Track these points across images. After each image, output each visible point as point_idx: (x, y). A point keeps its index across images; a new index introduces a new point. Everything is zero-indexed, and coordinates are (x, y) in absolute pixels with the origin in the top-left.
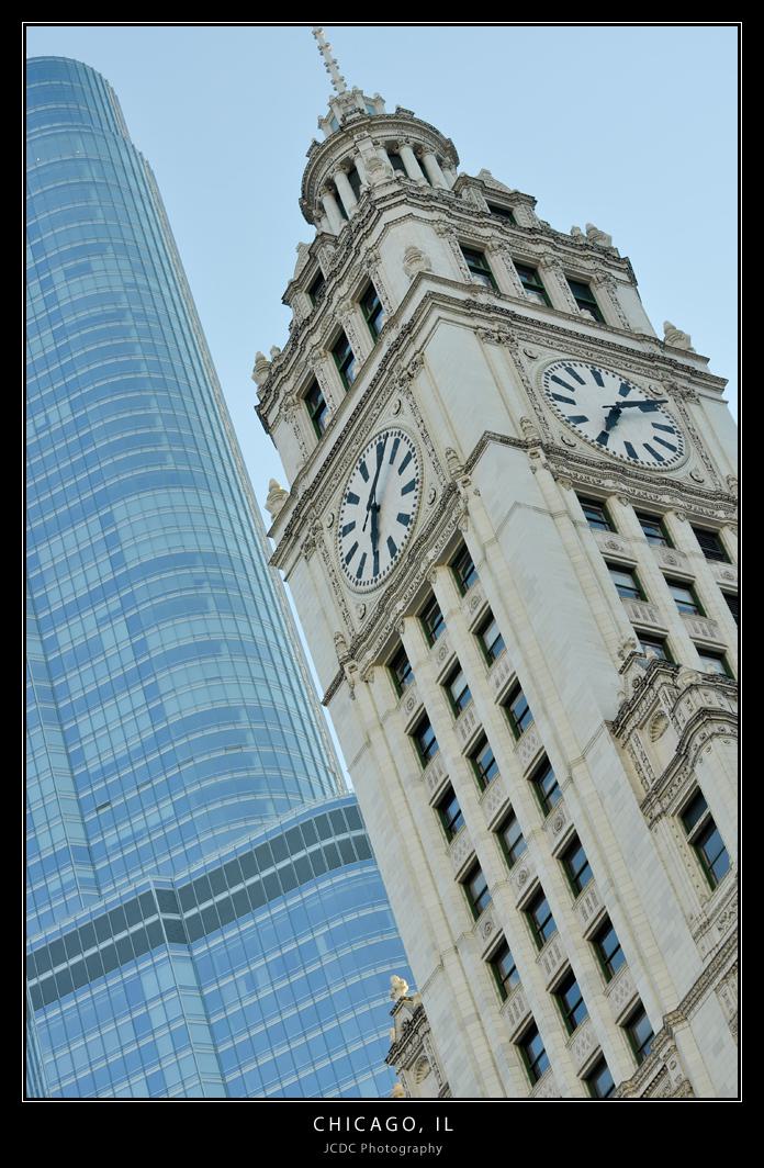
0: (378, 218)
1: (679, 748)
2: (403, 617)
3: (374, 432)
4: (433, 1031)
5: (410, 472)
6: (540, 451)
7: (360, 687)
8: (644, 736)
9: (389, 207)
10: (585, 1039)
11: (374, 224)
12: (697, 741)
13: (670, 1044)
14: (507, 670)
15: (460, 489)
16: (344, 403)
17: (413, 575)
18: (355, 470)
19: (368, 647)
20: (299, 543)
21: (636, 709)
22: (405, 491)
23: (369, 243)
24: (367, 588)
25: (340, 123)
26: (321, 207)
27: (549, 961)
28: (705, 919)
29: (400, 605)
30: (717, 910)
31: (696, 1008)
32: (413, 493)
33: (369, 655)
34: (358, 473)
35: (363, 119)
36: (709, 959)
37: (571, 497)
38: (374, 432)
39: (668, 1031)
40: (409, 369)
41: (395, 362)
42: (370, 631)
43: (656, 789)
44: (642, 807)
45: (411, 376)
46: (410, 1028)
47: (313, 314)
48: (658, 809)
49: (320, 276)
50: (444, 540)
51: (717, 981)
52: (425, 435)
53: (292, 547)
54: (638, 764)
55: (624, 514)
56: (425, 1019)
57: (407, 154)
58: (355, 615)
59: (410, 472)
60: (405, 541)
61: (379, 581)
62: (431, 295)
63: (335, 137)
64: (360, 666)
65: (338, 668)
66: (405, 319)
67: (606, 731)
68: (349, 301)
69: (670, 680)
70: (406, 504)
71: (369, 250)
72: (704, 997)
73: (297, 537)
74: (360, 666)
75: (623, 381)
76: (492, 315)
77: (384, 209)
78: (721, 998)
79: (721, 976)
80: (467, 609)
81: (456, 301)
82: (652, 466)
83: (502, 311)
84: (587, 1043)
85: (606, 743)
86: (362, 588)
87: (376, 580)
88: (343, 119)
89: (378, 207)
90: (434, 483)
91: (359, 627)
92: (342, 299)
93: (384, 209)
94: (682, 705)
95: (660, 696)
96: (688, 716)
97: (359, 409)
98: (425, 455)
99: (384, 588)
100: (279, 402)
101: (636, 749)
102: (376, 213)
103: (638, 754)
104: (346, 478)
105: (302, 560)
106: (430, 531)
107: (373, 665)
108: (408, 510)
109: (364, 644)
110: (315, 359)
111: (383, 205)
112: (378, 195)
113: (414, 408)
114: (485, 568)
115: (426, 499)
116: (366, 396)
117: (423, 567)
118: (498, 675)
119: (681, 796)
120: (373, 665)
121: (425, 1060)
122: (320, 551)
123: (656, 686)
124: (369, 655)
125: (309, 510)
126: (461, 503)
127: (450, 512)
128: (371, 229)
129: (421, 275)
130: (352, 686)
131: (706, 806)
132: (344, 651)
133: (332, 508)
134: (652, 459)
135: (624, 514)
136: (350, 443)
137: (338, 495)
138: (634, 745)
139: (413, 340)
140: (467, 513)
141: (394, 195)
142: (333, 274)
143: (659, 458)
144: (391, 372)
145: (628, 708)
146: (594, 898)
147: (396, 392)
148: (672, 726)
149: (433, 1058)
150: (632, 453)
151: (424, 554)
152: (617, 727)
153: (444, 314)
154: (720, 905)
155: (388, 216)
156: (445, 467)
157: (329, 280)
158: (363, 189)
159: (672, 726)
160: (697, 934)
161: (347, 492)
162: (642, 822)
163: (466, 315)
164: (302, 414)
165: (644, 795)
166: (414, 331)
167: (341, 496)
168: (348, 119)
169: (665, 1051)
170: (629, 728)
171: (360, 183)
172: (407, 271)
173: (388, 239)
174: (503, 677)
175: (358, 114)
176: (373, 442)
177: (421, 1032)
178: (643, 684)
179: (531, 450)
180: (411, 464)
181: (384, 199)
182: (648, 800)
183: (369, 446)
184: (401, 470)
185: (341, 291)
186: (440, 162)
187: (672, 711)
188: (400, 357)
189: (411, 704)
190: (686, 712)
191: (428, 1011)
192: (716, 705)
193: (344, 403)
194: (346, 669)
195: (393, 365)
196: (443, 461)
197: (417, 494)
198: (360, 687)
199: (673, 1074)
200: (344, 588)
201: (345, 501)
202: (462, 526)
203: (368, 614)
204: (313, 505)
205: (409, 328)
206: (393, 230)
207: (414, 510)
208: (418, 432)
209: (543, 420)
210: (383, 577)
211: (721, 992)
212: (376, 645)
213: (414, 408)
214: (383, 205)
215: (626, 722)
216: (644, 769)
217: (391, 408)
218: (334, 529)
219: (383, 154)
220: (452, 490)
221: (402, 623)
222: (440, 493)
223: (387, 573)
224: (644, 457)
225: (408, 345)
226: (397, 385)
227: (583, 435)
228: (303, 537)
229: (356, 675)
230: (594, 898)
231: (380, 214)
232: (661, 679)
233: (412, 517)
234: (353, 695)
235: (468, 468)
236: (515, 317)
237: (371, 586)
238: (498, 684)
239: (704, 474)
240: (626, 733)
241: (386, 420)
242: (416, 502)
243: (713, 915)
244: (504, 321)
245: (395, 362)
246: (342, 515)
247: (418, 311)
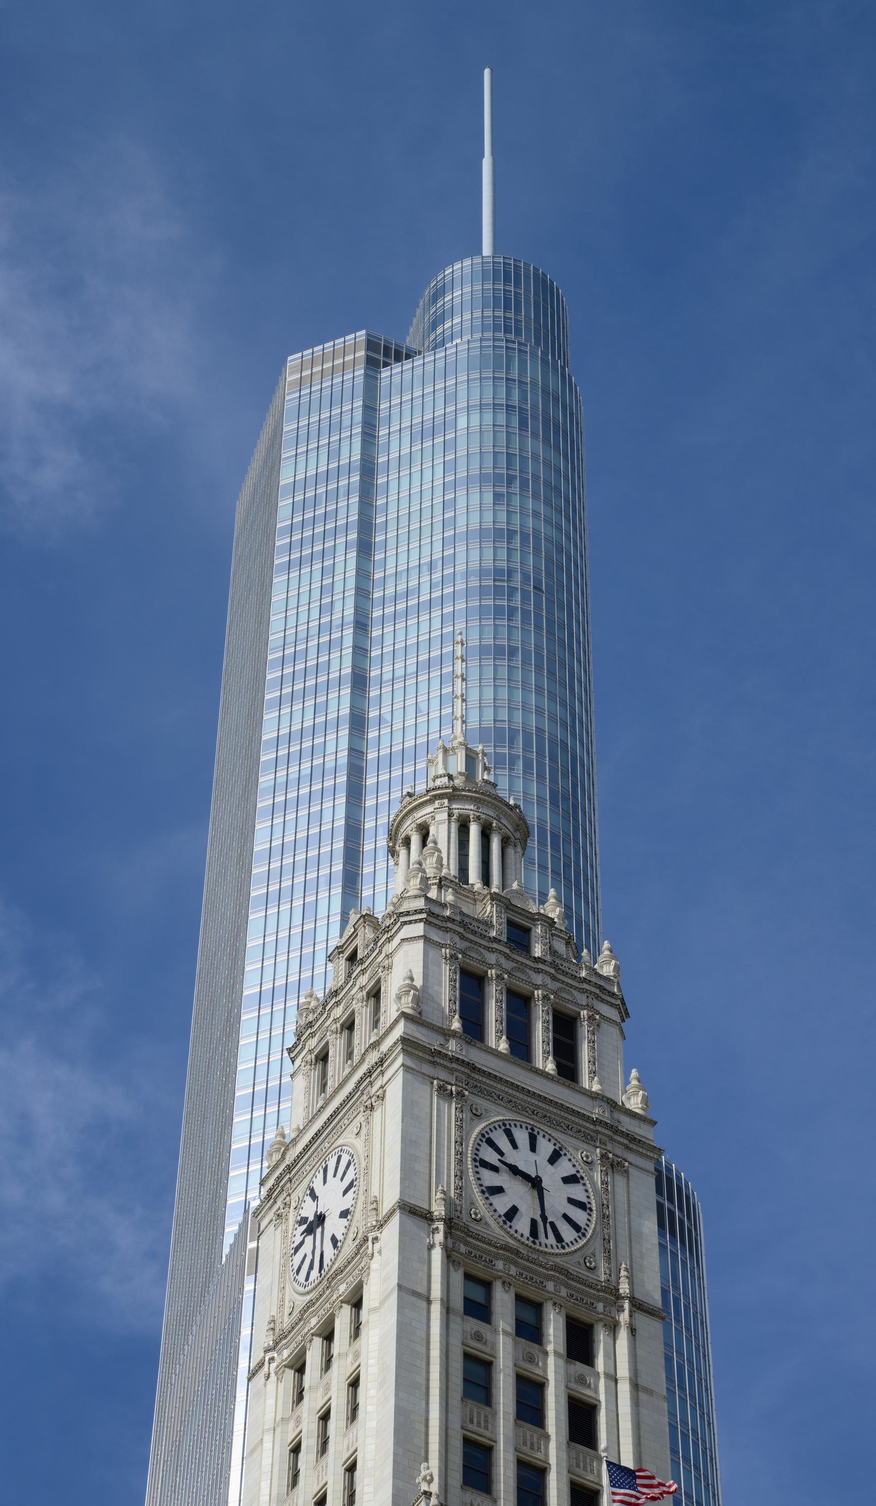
0: (399, 929)
2: (313, 1335)
9: (410, 922)
37: (458, 1277)
71: (387, 956)
76: (454, 1065)
77: (405, 923)
89: (402, 919)
102: (399, 924)
107: (286, 1366)
109: (284, 1342)
120: (286, 1366)
130: (268, 1377)
141: (416, 912)
163: (431, 1062)
181: (408, 913)
206: (406, 946)
212: (294, 1345)
244: (463, 1073)
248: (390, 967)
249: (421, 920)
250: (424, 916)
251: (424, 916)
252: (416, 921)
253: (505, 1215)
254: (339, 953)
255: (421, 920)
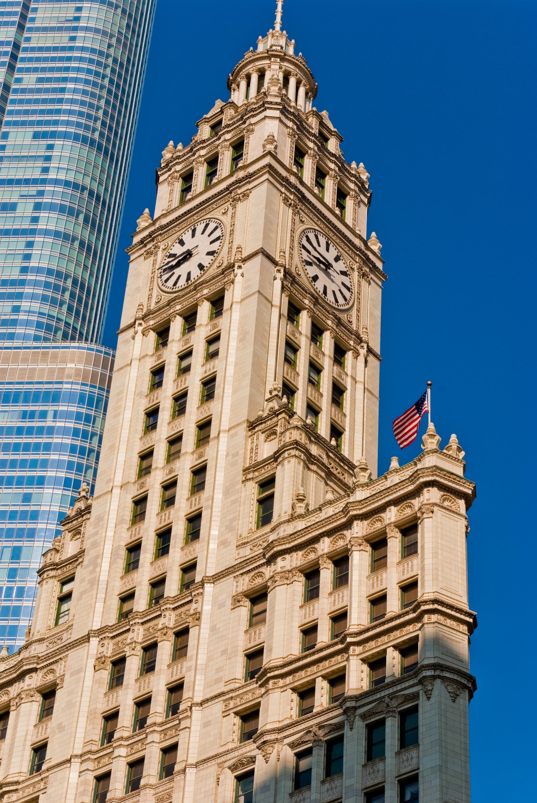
0: (263, 111)
1: (275, 453)
2: (177, 314)
3: (208, 216)
4: (91, 520)
5: (215, 246)
6: (282, 271)
7: (139, 336)
8: (262, 437)
9: (271, 108)
10: (161, 565)
11: (260, 112)
12: (286, 454)
13: (201, 590)
14: (213, 368)
15: (236, 268)
16: (201, 194)
17: (192, 297)
18: (189, 229)
19: (153, 319)
20: (144, 249)
21: (265, 422)
22: (209, 254)
23: (253, 120)
24: (166, 290)
25: (269, 47)
26: (238, 86)
27: (163, 518)
28: (246, 541)
29: (178, 307)
30: (254, 539)
31: (222, 580)
32: (211, 257)
33: (151, 322)
34: (190, 232)
35: (280, 52)
36: (239, 561)
37: (286, 300)
38: (208, 216)
39: (202, 584)
40: (241, 196)
41: (236, 188)
42: (157, 311)
43: (255, 466)
44: (244, 471)
45: (240, 199)
46: (81, 513)
47: (208, 139)
48: (250, 476)
49: (220, 122)
50: (215, 288)
51: (238, 573)
52: (232, 232)
53: (141, 249)
54: (252, 449)
55: (304, 319)
56: (90, 513)
57: (292, 81)
58: (154, 300)
59: (215, 246)
60: (196, 278)
61: (174, 290)
62: (270, 166)
63: (262, 53)
64: (144, 325)
65: (133, 320)
66: (251, 170)
67: (245, 425)
68: (228, 143)
69: (287, 418)
70: (206, 261)
71: (251, 124)
72: (228, 577)
73: (145, 246)
74: (144, 325)
75: (339, 254)
77: (268, 108)
78: (235, 583)
79: (241, 572)
80: (209, 327)
81: (280, 175)
82: (331, 304)
83: (298, 190)
84: (161, 567)
85: (243, 430)
86: (164, 288)
87: (173, 289)
88: (271, 47)
89: (266, 105)
90: (224, 258)
91: (153, 306)
92: (226, 140)
93: (268, 108)
94: (288, 433)
95: (279, 423)
96: (288, 440)
97: (207, 200)
98: (227, 242)
99: (175, 295)
100: (169, 173)
101: (255, 441)
103: (255, 444)
104: (183, 230)
105: (142, 258)
106: (210, 280)
107: (151, 329)
108: (205, 264)
109: (151, 316)
110: (197, 163)
111: (269, 106)
112: (269, 99)
113: (233, 217)
114: (229, 312)
115: (216, 264)
116: (213, 197)
117: (199, 295)
118: (208, 368)
119: (264, 474)
120: (151, 329)
121: (79, 533)
122: (152, 258)
123: (280, 417)
124: (151, 322)
125: (158, 236)
126: (232, 276)
127: (225, 277)
128: (257, 114)
129: (270, 153)
131: (274, 487)
132: (140, 314)
133: (169, 241)
134: (333, 300)
135: (304, 319)
136: (194, 215)
137: (175, 236)
138: (255, 438)
139: (249, 182)
140: (233, 282)
141: (276, 104)
142: (228, 126)
143: (337, 301)
144: (231, 193)
145: (261, 420)
146: (199, 500)
147: (229, 203)
148: (277, 440)
149: (84, 533)
150: (325, 292)
151: (202, 289)
152: (252, 426)
153: (271, 179)
154: (257, 538)
155: (268, 113)
156: (234, 254)
157: (224, 128)
158: (263, 90)
159: (277, 440)
160: (239, 545)
161: (181, 238)
162: (241, 478)
164: (178, 185)
165: (248, 465)
166: (252, 178)
167: (176, 237)
168: (274, 48)
169: (197, 592)
170: (257, 429)
171: (263, 86)
172: (264, 146)
173: (262, 124)
174: (210, 369)
175: (279, 48)
176: (205, 221)
177: (84, 518)
178: (275, 413)
179: (278, 268)
180: (218, 243)
181: (271, 103)
182: (248, 469)
183: (202, 222)
184: (212, 243)
185: (228, 136)
186: (307, 94)
187: (282, 433)
188: (239, 187)
189: (159, 357)
190: (288, 437)
191: (93, 510)
192: (303, 441)
193: (201, 194)
194: (137, 322)
195: (234, 189)
196: (234, 250)
197: (214, 258)
198: (139, 336)
199: (193, 606)
200: (155, 283)
201: (177, 241)
202: (227, 287)
203: (161, 303)
204: (161, 234)
205: (250, 176)
206: (267, 121)
207: (208, 265)
208: (229, 228)
209: (291, 255)
210: (177, 289)
211: (237, 579)
213: (233, 216)
214: (269, 106)
215: (257, 426)
216: (254, 453)
217: (222, 210)
218: (165, 252)
219: (281, 76)
220: (231, 267)
221: (175, 317)
222: (225, 264)
223: (180, 288)
224: (330, 297)
225: (246, 183)
226: (231, 200)
227: (306, 272)
228: (148, 247)
229: (140, 329)
230: (199, 500)
231: (265, 110)
232: (283, 415)
233: (205, 268)
234: (133, 338)
235: (244, 260)
236: (304, 197)
237: (169, 290)
238: (206, 372)
239: (354, 319)
240: (254, 431)
241: (217, 214)
242: (211, 262)
243: (251, 541)
245: (236, 188)
246: (172, 247)
247: (259, 170)
248: (253, 130)
249: (278, 109)
250: (281, 107)
251: (281, 107)
252: (275, 109)
253: (313, 278)
254: (206, 122)
255: (278, 109)
